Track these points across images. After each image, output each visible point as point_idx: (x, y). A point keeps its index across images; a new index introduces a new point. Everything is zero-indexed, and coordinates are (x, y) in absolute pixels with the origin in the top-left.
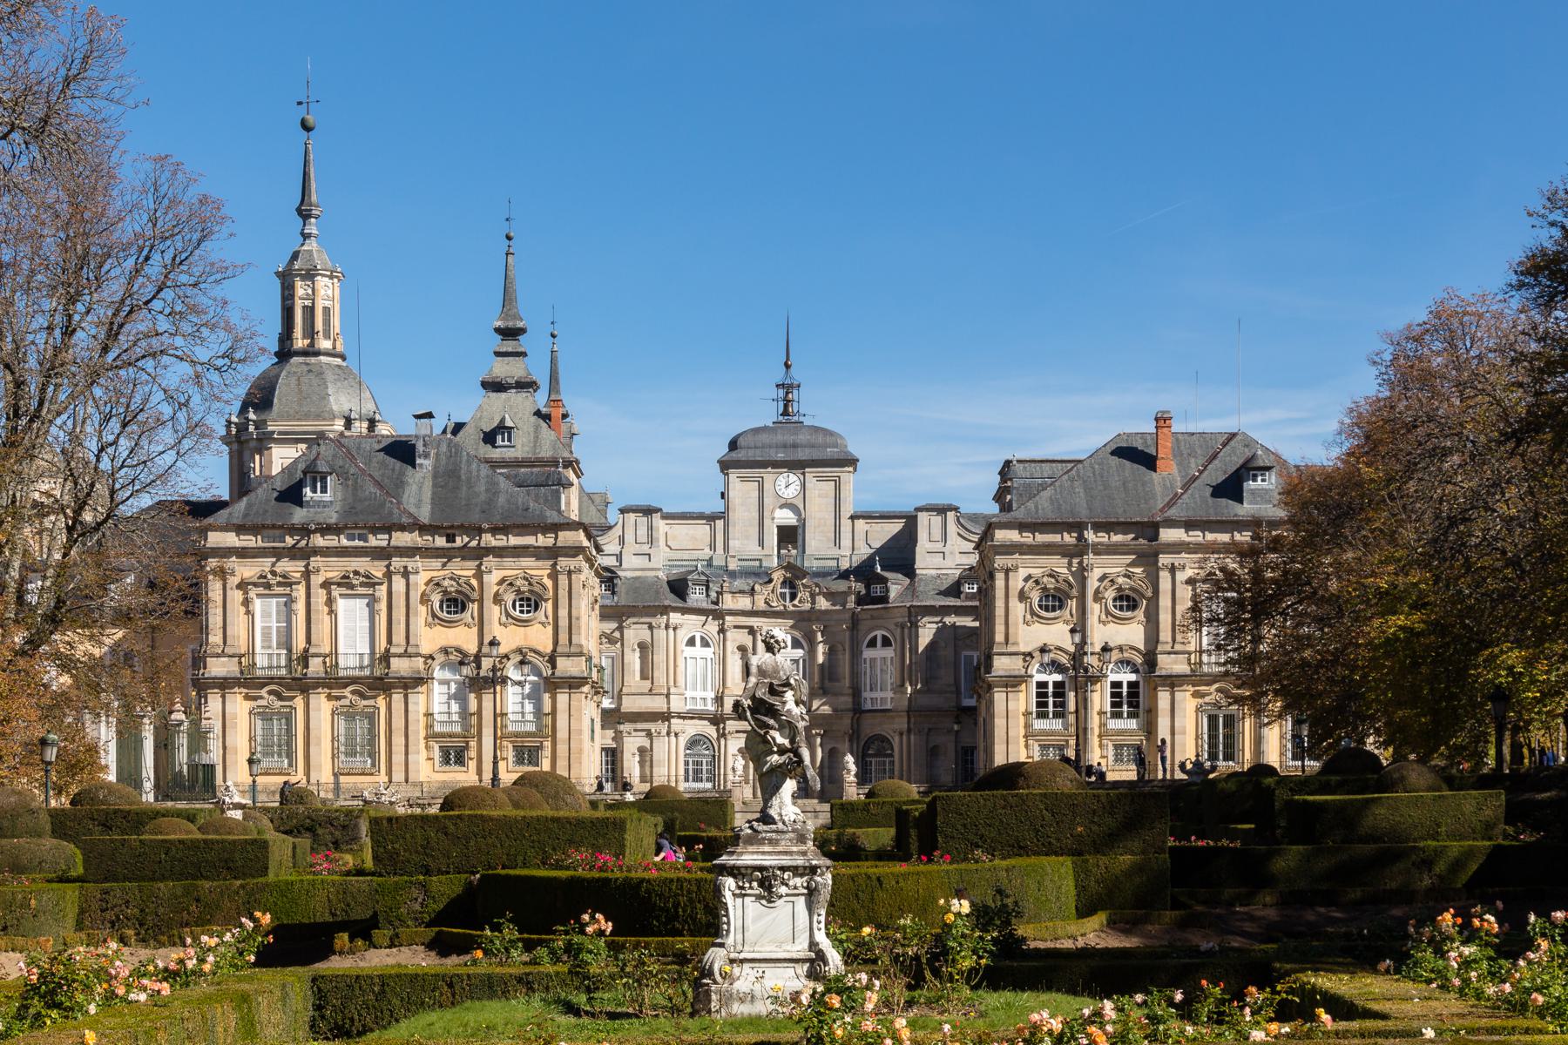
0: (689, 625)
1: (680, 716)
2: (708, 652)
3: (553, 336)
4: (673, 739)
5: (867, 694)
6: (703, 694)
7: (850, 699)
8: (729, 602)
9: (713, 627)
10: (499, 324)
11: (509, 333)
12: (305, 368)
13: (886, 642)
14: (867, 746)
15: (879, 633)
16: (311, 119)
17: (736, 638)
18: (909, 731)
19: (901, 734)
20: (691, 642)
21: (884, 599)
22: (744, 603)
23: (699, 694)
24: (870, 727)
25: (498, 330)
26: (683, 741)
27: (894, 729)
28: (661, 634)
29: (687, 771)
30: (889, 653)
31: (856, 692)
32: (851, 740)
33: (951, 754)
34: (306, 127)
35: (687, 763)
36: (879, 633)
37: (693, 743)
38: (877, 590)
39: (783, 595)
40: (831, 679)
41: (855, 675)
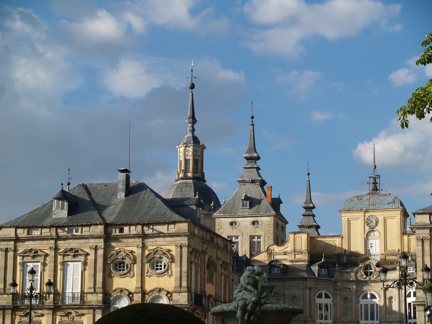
12: (185, 185)
39: (366, 274)
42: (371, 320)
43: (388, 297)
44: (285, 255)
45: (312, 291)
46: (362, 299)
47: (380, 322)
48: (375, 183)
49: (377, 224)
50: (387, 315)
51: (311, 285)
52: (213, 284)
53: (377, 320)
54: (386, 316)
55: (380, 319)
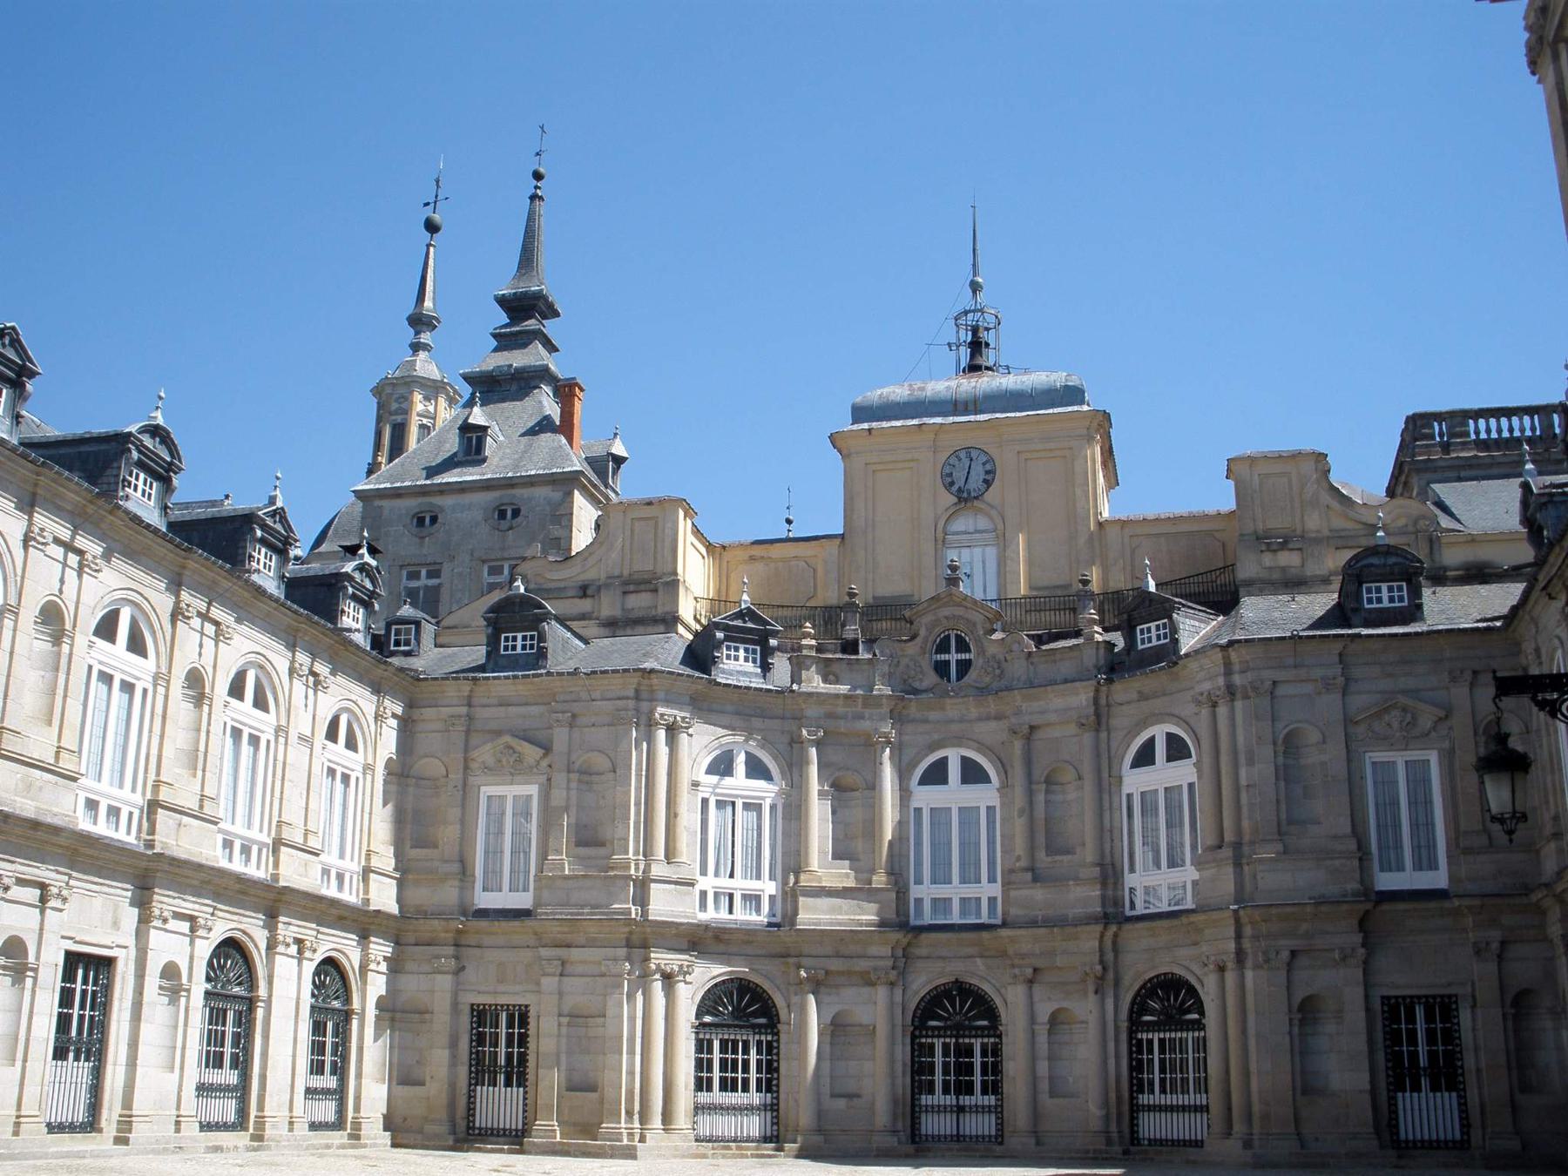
3: (789, 522)
6: (752, 885)
7: (1096, 892)
13: (1177, 750)
14: (1138, 1007)
15: (1159, 732)
16: (437, 217)
18: (1240, 956)
19: (1221, 969)
21: (1168, 653)
23: (741, 884)
25: (502, 301)
26: (688, 997)
29: (702, 1065)
30: (1183, 773)
31: (1110, 874)
33: (1356, 1016)
34: (432, 227)
35: (702, 1046)
36: (1159, 732)
38: (1150, 635)
40: (1051, 850)
41: (1105, 833)
42: (963, 881)
43: (1039, 773)
44: (585, 595)
46: (923, 782)
48: (977, 346)
49: (988, 483)
50: (1041, 855)
53: (992, 880)
54: (1032, 857)
55: (1009, 872)
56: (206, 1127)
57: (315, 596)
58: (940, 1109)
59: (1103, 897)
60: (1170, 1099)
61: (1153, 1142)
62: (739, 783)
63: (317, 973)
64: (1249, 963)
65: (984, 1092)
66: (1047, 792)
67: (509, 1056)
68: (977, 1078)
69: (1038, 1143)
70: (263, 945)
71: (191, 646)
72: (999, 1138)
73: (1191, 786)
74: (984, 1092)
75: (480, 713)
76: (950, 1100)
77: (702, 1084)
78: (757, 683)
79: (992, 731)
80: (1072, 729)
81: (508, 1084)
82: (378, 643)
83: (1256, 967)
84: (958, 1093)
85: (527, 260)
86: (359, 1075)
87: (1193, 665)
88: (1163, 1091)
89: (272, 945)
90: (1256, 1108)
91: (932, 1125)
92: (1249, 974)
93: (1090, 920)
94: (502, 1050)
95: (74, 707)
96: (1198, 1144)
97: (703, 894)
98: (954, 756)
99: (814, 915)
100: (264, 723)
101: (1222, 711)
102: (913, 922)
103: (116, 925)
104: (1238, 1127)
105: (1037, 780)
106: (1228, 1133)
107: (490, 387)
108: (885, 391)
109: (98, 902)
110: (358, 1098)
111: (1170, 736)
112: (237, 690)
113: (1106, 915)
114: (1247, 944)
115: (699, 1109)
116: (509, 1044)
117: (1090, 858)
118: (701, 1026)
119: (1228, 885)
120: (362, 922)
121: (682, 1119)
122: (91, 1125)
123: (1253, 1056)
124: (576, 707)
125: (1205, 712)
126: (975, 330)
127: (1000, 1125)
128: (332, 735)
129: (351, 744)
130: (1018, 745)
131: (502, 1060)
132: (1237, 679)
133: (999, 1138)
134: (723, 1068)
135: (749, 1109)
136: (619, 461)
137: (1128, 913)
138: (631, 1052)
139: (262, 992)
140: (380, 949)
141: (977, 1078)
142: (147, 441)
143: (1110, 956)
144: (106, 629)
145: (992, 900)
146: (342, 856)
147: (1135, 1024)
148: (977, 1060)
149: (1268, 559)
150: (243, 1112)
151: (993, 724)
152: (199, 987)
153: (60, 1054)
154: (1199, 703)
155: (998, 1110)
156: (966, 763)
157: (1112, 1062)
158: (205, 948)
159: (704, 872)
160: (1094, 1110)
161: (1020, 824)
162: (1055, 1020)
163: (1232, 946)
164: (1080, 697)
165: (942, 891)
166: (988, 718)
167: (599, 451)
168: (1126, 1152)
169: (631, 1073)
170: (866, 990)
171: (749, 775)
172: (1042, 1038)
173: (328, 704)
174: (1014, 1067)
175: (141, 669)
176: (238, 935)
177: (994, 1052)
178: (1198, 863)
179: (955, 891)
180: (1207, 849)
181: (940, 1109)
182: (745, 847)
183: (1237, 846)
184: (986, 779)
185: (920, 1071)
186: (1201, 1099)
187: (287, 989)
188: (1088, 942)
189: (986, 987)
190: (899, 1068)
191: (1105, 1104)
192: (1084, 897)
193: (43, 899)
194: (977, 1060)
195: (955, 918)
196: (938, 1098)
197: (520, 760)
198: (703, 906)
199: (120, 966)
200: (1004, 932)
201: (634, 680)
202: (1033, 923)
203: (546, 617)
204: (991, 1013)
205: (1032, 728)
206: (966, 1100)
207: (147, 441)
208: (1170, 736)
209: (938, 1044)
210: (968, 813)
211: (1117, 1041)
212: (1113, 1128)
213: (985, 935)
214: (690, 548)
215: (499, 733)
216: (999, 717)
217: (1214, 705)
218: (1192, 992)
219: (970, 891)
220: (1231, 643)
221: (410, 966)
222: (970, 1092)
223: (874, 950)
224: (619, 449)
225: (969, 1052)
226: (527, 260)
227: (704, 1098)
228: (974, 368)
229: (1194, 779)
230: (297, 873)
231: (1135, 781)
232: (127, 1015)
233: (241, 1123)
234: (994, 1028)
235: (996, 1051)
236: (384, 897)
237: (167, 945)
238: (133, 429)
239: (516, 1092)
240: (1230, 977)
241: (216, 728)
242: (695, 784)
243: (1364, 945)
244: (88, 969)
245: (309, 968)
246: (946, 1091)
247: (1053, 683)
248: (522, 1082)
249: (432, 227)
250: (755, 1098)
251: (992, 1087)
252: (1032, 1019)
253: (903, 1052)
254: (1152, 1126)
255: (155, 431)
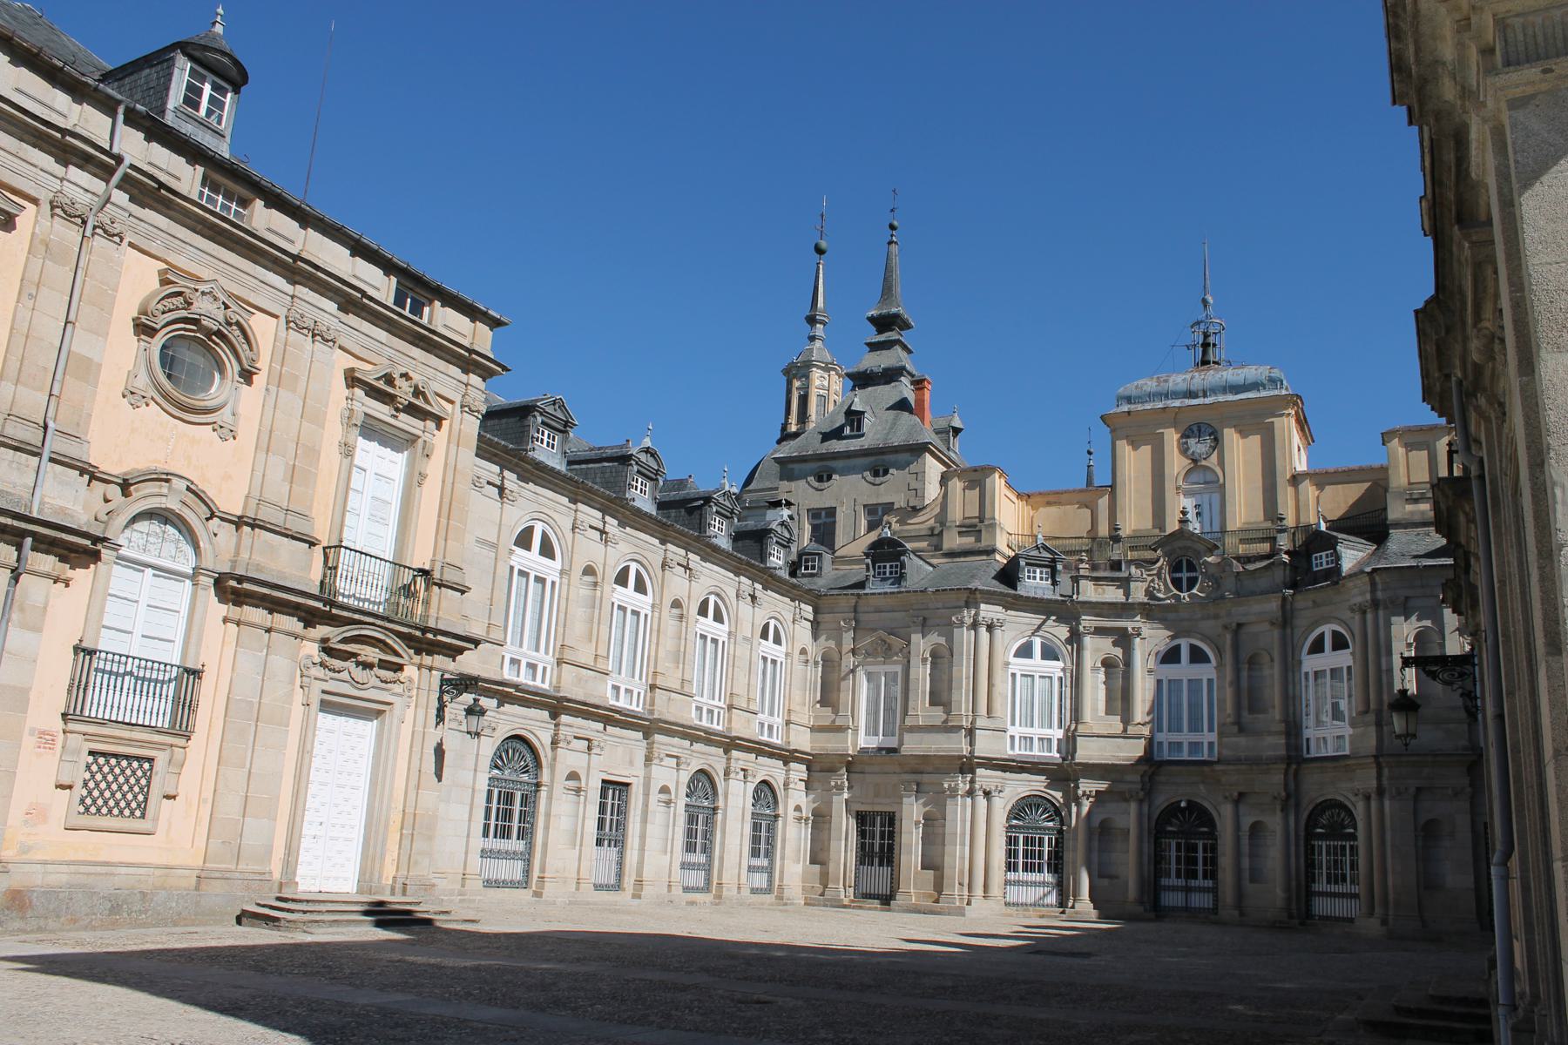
0: (1016, 626)
1: (992, 764)
2: (1055, 668)
4: (982, 802)
5: (1310, 732)
6: (1046, 732)
8: (1089, 592)
9: (1063, 632)
10: (874, 313)
11: (883, 323)
13: (1339, 643)
14: (1312, 821)
15: (1327, 629)
16: (823, 244)
17: (1096, 649)
18: (1380, 792)
19: (1368, 798)
20: (1025, 651)
21: (1334, 573)
22: (1113, 594)
23: (1037, 731)
24: (1316, 788)
25: (872, 320)
27: (1351, 790)
28: (965, 636)
29: (1011, 854)
30: (1344, 659)
31: (1293, 729)
32: (1284, 809)
35: (1011, 841)
36: (1327, 629)
37: (1021, 809)
40: (1252, 710)
41: (1291, 700)
43: (1244, 656)
45: (998, 632)
47: (1221, 735)
50: (1245, 713)
51: (990, 615)
52: (228, 433)
53: (1211, 729)
55: (1221, 725)
56: (686, 889)
57: (751, 545)
58: (1174, 889)
59: (1288, 746)
60: (1333, 888)
61: (1322, 918)
62: (1037, 663)
63: (756, 790)
64: (1387, 796)
65: (1205, 877)
66: (1250, 669)
67: (882, 846)
68: (1200, 868)
69: (1242, 914)
70: (722, 774)
71: (677, 584)
72: (1215, 910)
73: (1349, 668)
74: (1205, 877)
75: (862, 617)
76: (1181, 882)
77: (1011, 867)
78: (1049, 595)
79: (1208, 626)
80: (1266, 626)
81: (881, 864)
82: (794, 569)
83: (1392, 798)
84: (1187, 878)
85: (887, 291)
86: (783, 858)
87: (1350, 584)
88: (1329, 882)
89: (727, 773)
90: (1391, 897)
91: (1171, 899)
92: (1387, 803)
93: (1275, 760)
94: (877, 841)
95: (604, 629)
96: (1351, 920)
97: (1012, 737)
98: (1185, 644)
99: (1088, 752)
100: (721, 631)
101: (1369, 616)
102: (1157, 758)
103: (631, 763)
104: (1378, 910)
105: (1244, 663)
106: (1371, 913)
107: (862, 380)
108: (1140, 382)
109: (620, 750)
110: (782, 872)
111: (1335, 634)
112: (703, 611)
113: (1289, 757)
114: (1385, 782)
115: (1007, 883)
116: (882, 838)
117: (1278, 717)
118: (1010, 828)
119: (1371, 742)
120: (787, 756)
121: (996, 890)
122: (618, 886)
123: (1389, 861)
124: (926, 613)
125: (1357, 617)
126: (1206, 336)
127: (1216, 901)
128: (764, 635)
129: (777, 641)
130: (1228, 637)
131: (877, 849)
132: (1380, 595)
133: (1215, 910)
134: (1026, 856)
135: (1043, 884)
136: (957, 431)
137: (1306, 756)
138: (963, 844)
139: (721, 803)
140: (799, 771)
141: (1200, 868)
142: (643, 457)
143: (1292, 786)
144: (622, 579)
145: (1211, 744)
146: (771, 714)
147: (1310, 835)
148: (1200, 855)
149: (1409, 508)
150: (708, 880)
151: (1211, 623)
152: (682, 801)
153: (599, 842)
154: (1353, 610)
155: (1214, 891)
156: (1193, 648)
157: (1293, 860)
158: (685, 777)
159: (1013, 724)
160: (1279, 892)
161: (1229, 693)
162: (1256, 828)
163: (1374, 783)
164: (1272, 605)
165: (1175, 737)
166: (1208, 618)
167: (943, 424)
168: (1302, 924)
169: (962, 858)
170: (1124, 805)
171: (1044, 657)
172: (1245, 841)
173: (761, 616)
174: (1226, 861)
175: (643, 603)
176: (706, 767)
177: (1213, 849)
178: (1353, 725)
179: (1185, 737)
180: (1359, 714)
181: (1174, 889)
182: (1041, 704)
183: (1379, 713)
184: (1207, 660)
185: (1158, 858)
186: (1355, 889)
187: (737, 800)
188: (1277, 778)
189: (1206, 804)
190: (1146, 858)
191: (1288, 889)
192: (1274, 744)
193: (589, 748)
194: (1200, 855)
195: (1185, 756)
196: (1173, 881)
197: (889, 648)
198: (1012, 747)
199: (634, 789)
200: (1218, 767)
201: (964, 596)
202: (1237, 761)
203: (904, 552)
204: (1211, 823)
205: (1239, 625)
206: (1193, 883)
207: (643, 457)
208: (1335, 634)
209: (1173, 844)
210: (1194, 684)
211: (1297, 845)
212: (1294, 906)
213: (1206, 769)
214: (1005, 500)
215: (874, 630)
216: (1216, 617)
217: (1364, 613)
218: (1350, 814)
219: (1195, 737)
220: (1374, 570)
221: (816, 785)
222: (1195, 877)
223: (1129, 778)
224: (957, 423)
225: (1194, 849)
226: (887, 291)
227: (1012, 876)
228: (1205, 362)
229: (1351, 663)
230: (743, 727)
231: (1311, 663)
232: (638, 819)
233: (707, 888)
234: (1212, 834)
235: (1214, 849)
236: (802, 741)
237: (664, 774)
238: (634, 451)
239: (886, 870)
240: (1374, 804)
241: (690, 637)
242: (1007, 664)
243: (1471, 785)
244: (615, 789)
245: (751, 787)
246: (1178, 876)
247: (1253, 593)
248: (890, 862)
249: (820, 251)
250: (1048, 877)
251: (1212, 874)
252: (1237, 827)
253: (1147, 848)
254: (1322, 906)
255: (647, 451)
